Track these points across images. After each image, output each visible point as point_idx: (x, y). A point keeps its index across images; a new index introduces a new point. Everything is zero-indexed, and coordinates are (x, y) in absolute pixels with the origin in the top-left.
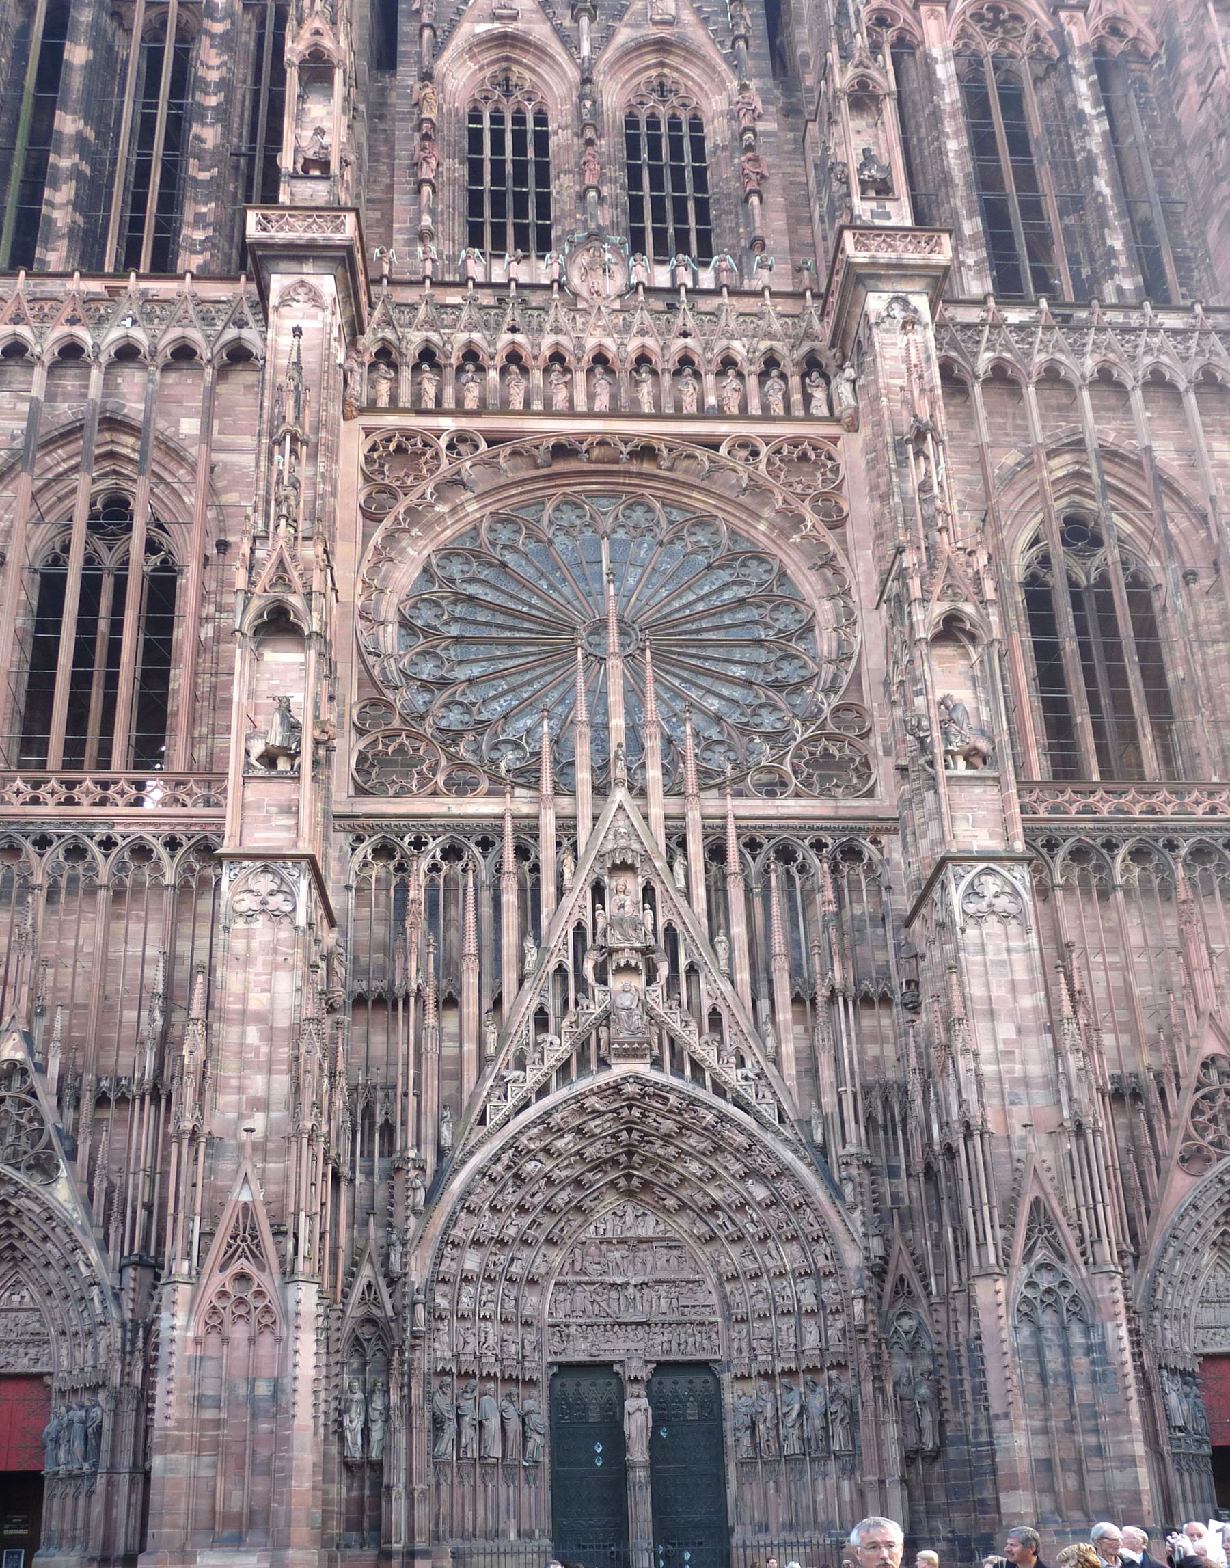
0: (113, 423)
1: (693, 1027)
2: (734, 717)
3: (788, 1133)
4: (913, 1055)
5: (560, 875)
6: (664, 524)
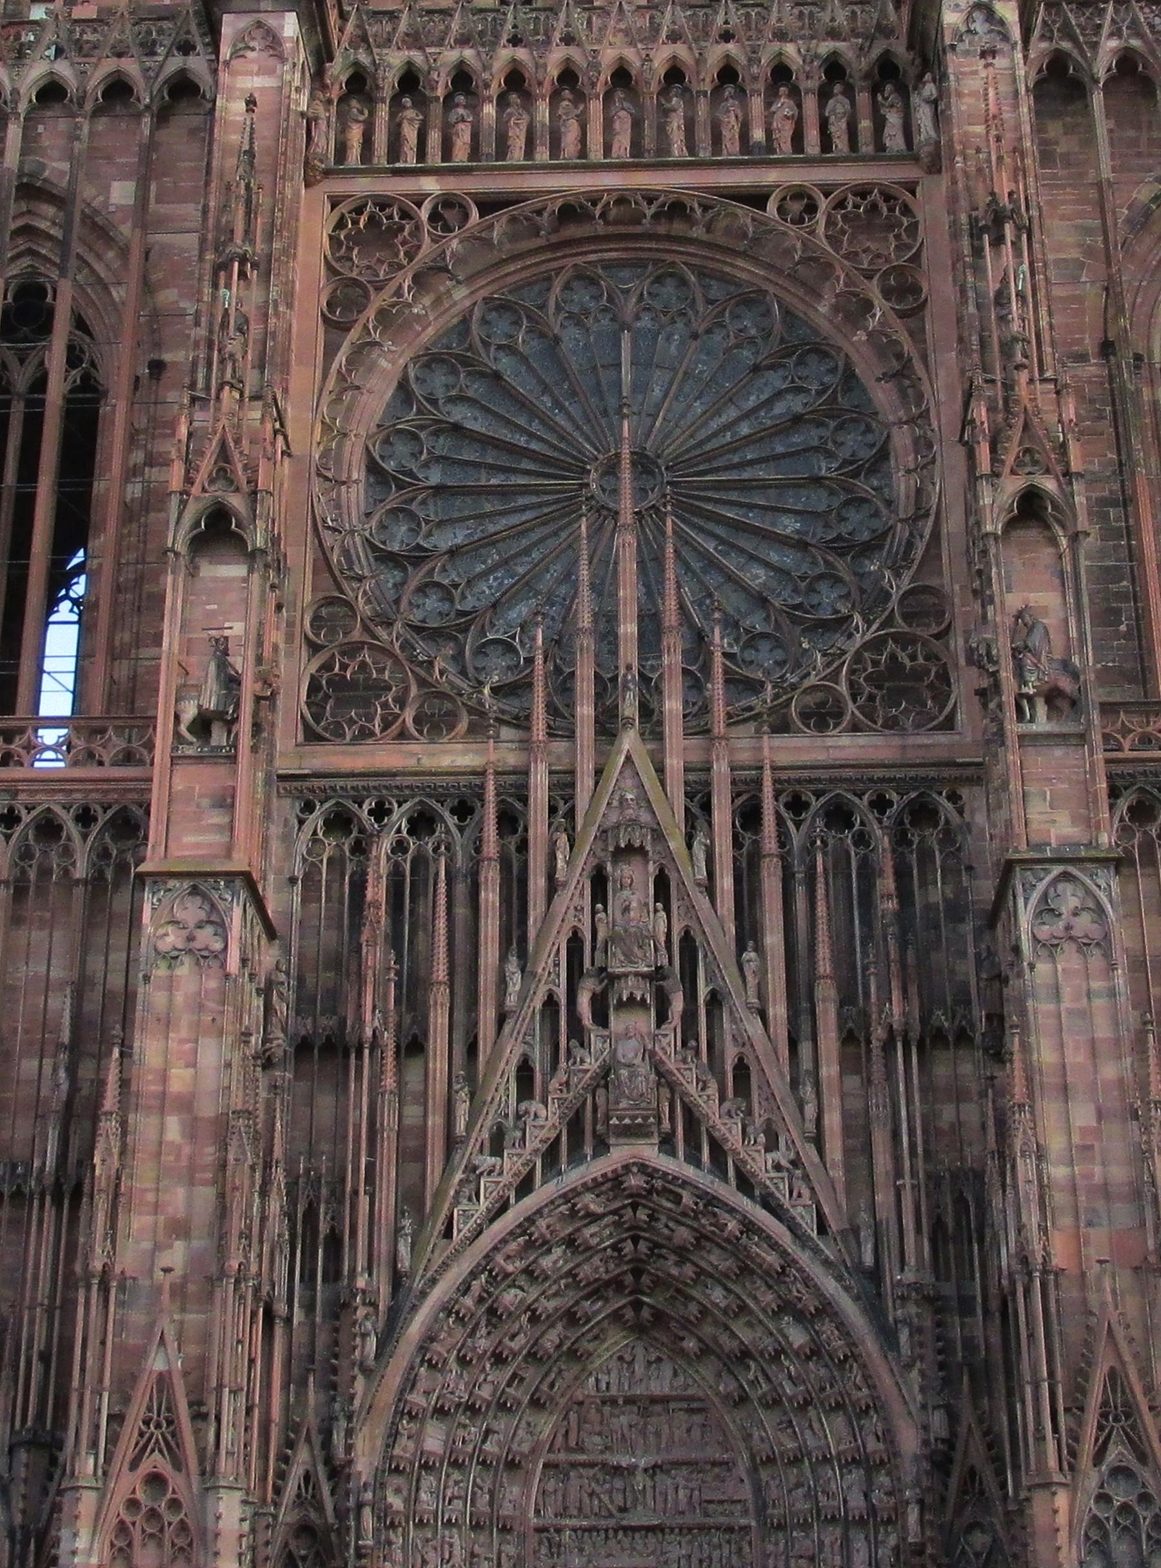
1: (713, 1089)
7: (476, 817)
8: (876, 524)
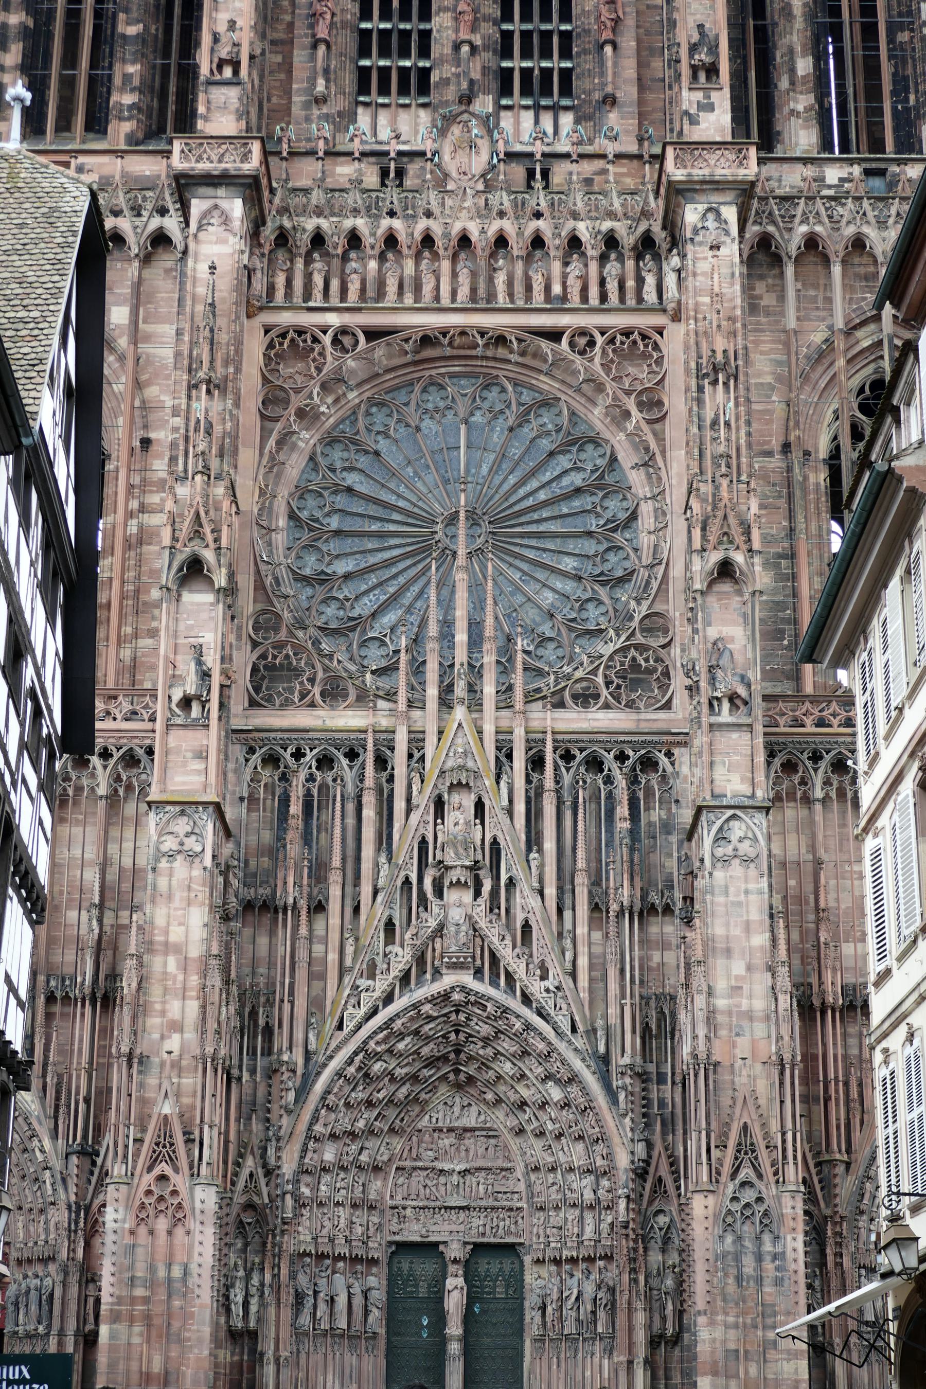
1: (508, 940)
4: (682, 970)
5: (409, 786)
7: (361, 759)
8: (627, 564)
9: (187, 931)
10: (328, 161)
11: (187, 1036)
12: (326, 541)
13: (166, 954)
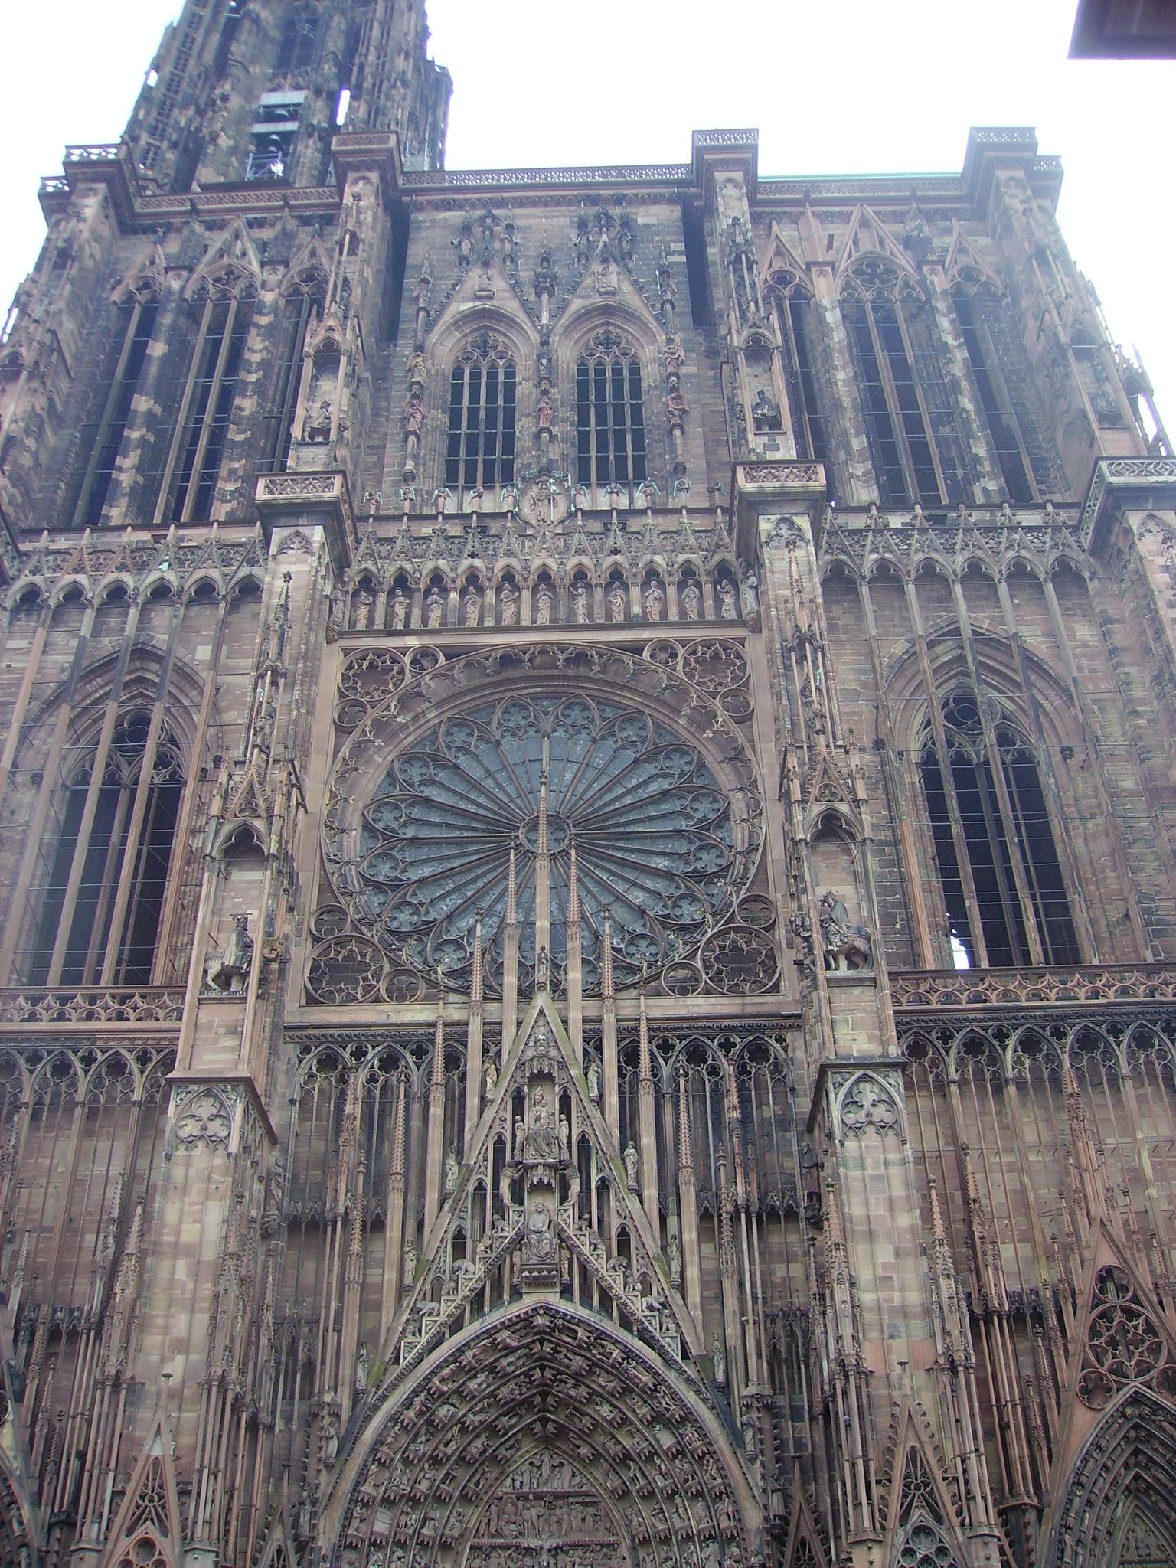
0: (143, 653)
2: (656, 909)
3: (691, 1371)
5: (484, 1083)
6: (598, 722)
8: (720, 862)
9: (202, 1231)
10: (414, 525)
11: (193, 1357)
12: (402, 850)
13: (175, 1257)
